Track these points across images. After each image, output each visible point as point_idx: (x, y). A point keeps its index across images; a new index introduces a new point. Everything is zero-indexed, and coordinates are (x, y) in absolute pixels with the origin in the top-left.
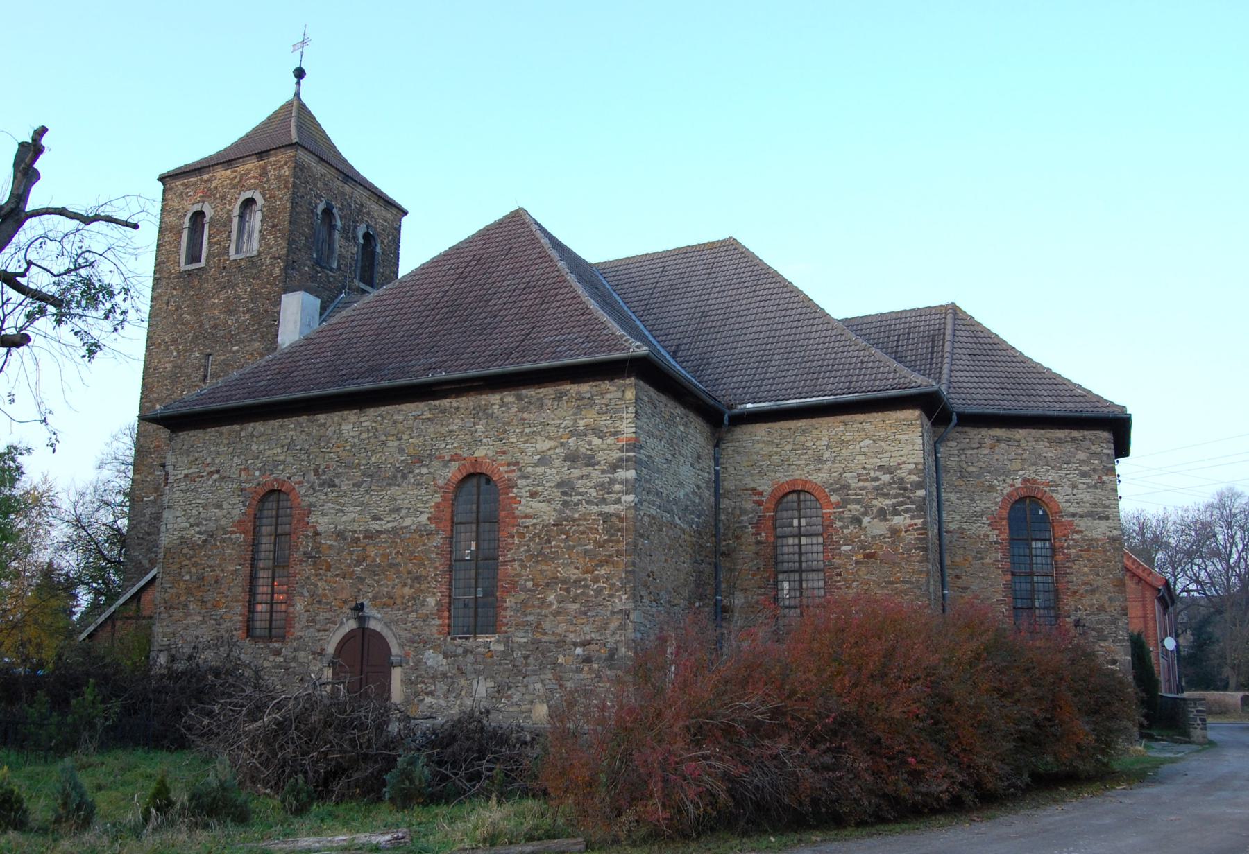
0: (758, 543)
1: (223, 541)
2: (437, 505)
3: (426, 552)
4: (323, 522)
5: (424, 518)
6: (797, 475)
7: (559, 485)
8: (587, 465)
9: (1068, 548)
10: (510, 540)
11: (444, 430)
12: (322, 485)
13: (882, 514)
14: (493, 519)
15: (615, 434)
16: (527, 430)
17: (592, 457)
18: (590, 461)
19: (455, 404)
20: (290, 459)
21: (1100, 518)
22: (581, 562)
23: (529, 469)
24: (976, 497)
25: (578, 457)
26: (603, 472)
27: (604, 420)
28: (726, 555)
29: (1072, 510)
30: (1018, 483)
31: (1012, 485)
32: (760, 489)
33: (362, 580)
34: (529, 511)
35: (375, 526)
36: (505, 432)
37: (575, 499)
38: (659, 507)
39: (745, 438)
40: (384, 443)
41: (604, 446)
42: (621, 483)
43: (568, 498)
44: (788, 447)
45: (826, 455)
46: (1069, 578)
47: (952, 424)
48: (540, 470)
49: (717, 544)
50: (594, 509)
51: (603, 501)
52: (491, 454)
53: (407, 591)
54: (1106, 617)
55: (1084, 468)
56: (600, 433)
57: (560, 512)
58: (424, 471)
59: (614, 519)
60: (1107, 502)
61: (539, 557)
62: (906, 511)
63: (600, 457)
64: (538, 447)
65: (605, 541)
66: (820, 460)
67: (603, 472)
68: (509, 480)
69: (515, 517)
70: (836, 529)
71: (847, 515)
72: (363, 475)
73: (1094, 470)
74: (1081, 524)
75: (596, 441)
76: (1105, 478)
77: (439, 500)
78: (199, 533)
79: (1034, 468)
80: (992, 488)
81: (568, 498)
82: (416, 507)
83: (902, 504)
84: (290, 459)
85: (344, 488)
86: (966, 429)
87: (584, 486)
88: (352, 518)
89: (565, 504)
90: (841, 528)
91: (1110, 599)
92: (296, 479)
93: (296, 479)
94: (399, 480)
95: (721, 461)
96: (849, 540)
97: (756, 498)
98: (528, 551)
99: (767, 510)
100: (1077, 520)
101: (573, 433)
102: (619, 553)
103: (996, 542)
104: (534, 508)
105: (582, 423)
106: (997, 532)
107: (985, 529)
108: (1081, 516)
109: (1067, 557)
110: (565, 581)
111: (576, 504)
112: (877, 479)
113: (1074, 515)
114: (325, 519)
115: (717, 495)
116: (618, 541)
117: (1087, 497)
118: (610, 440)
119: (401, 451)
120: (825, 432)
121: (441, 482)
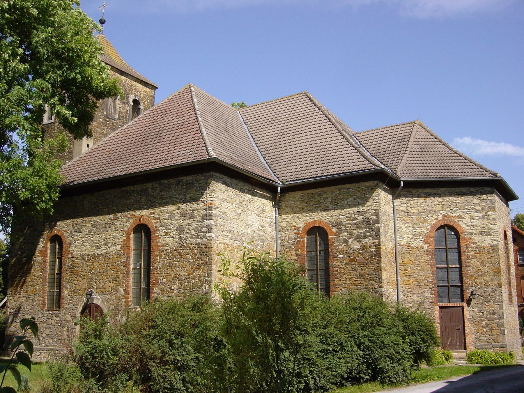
5: (118, 247)
9: (468, 252)
13: (358, 238)
16: (164, 201)
18: (192, 216)
21: (486, 235)
24: (416, 226)
29: (471, 231)
30: (440, 217)
31: (436, 219)
34: (164, 242)
35: (99, 252)
36: (154, 202)
37: (185, 236)
38: (232, 239)
44: (312, 204)
47: (400, 188)
48: (170, 221)
51: (198, 237)
54: (489, 289)
55: (478, 208)
58: (119, 223)
60: (491, 226)
62: (370, 236)
63: (196, 213)
68: (156, 227)
69: (158, 246)
71: (341, 238)
73: (483, 209)
74: (476, 238)
76: (489, 213)
79: (448, 209)
80: (425, 221)
83: (368, 232)
86: (411, 189)
88: (88, 248)
91: (492, 279)
100: (473, 237)
103: (427, 250)
106: (428, 245)
107: (422, 244)
108: (476, 234)
109: (468, 257)
112: (355, 219)
113: (471, 234)
114: (77, 249)
117: (479, 224)
120: (330, 195)
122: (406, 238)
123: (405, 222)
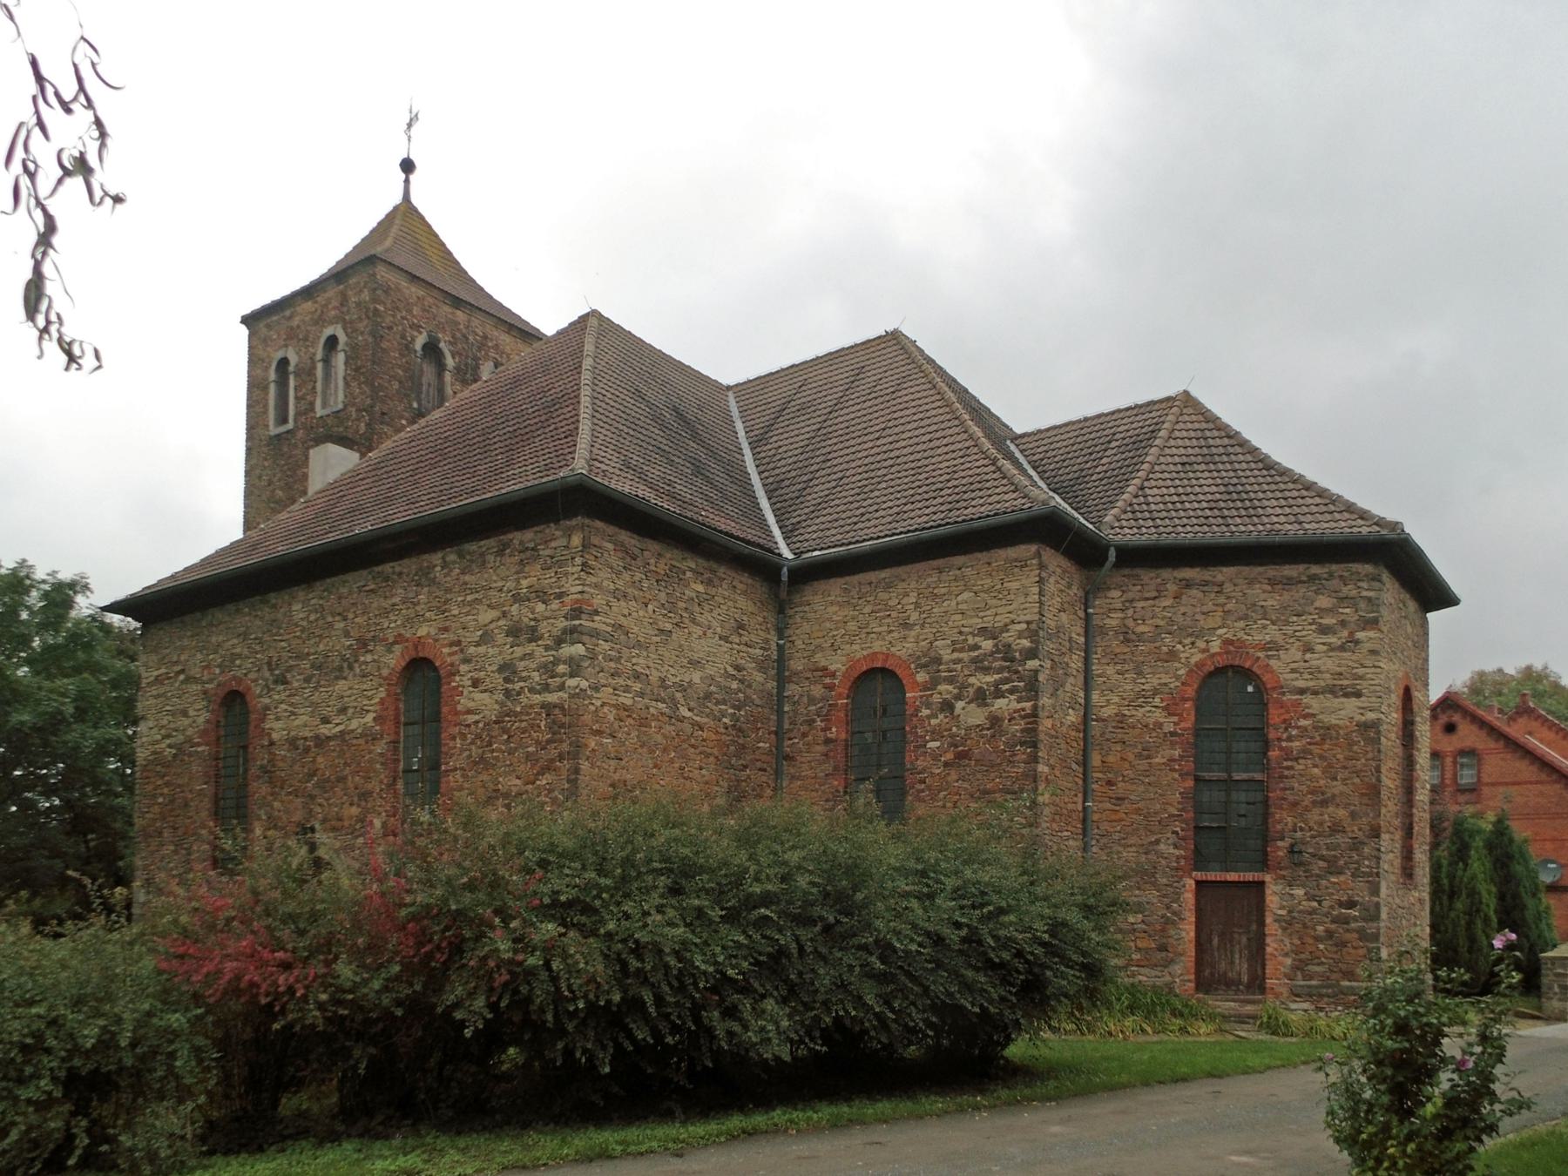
0: (828, 741)
1: (190, 755)
2: (382, 702)
3: (371, 761)
4: (277, 729)
5: (369, 718)
6: (878, 646)
7: (501, 669)
8: (530, 641)
9: (1290, 739)
10: (451, 744)
11: (386, 604)
12: (276, 682)
13: (981, 697)
14: (437, 717)
15: (560, 596)
16: (469, 598)
17: (534, 629)
18: (534, 636)
19: (397, 569)
20: (246, 652)
21: (1346, 695)
22: (523, 768)
23: (472, 650)
24: (1146, 669)
25: (520, 630)
26: (547, 648)
27: (548, 579)
28: (787, 758)
29: (1301, 684)
30: (1215, 646)
31: (1204, 651)
32: (832, 668)
33: (312, 797)
34: (471, 705)
35: (325, 730)
36: (445, 603)
37: (517, 686)
38: (642, 694)
39: (817, 598)
40: (331, 625)
41: (547, 614)
42: (565, 663)
43: (510, 686)
44: (867, 610)
45: (914, 617)
46: (828, 767)
47: (1108, 565)
48: (482, 649)
49: (779, 746)
50: (537, 698)
51: (546, 688)
52: (433, 632)
53: (355, 810)
54: (1340, 839)
55: (1328, 621)
56: (542, 595)
57: (502, 704)
58: (369, 658)
59: (557, 711)
60: (1361, 671)
61: (482, 763)
62: (1012, 691)
63: (544, 628)
64: (480, 618)
65: (549, 742)
66: (906, 625)
67: (547, 648)
68: (452, 665)
69: (457, 713)
70: (922, 720)
71: (936, 699)
72: (313, 666)
73: (1343, 623)
74: (1314, 703)
75: (540, 607)
76: (1360, 635)
77: (383, 695)
78: (170, 746)
79: (1242, 624)
80: (1172, 655)
81: (510, 686)
82: (362, 703)
83: (1006, 681)
84: (246, 652)
85: (296, 684)
86: (1139, 571)
87: (526, 669)
88: (303, 724)
89: (507, 693)
90: (929, 717)
91: (1353, 815)
92: (252, 676)
93: (252, 676)
94: (346, 672)
95: (788, 632)
96: (936, 734)
97: (828, 680)
98: (470, 756)
99: (840, 696)
100: (1307, 699)
101: (517, 598)
102: (561, 757)
103: (1172, 734)
104: (476, 702)
105: (525, 583)
106: (1175, 719)
107: (1159, 715)
108: (1315, 693)
109: (1288, 755)
110: (506, 795)
111: (519, 694)
112: (976, 647)
113: (1302, 691)
114: (280, 725)
115: (782, 681)
116: (561, 741)
117: (1329, 664)
118: (555, 605)
119: (347, 634)
120: (913, 585)
121: (385, 672)
122: (1116, 699)
123: (1114, 658)
